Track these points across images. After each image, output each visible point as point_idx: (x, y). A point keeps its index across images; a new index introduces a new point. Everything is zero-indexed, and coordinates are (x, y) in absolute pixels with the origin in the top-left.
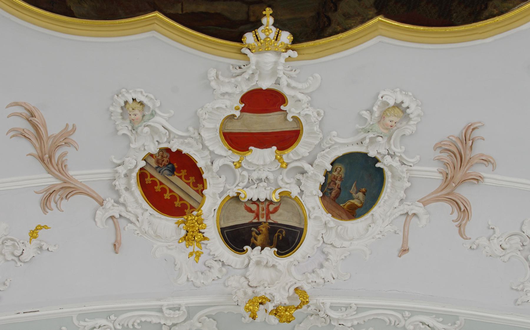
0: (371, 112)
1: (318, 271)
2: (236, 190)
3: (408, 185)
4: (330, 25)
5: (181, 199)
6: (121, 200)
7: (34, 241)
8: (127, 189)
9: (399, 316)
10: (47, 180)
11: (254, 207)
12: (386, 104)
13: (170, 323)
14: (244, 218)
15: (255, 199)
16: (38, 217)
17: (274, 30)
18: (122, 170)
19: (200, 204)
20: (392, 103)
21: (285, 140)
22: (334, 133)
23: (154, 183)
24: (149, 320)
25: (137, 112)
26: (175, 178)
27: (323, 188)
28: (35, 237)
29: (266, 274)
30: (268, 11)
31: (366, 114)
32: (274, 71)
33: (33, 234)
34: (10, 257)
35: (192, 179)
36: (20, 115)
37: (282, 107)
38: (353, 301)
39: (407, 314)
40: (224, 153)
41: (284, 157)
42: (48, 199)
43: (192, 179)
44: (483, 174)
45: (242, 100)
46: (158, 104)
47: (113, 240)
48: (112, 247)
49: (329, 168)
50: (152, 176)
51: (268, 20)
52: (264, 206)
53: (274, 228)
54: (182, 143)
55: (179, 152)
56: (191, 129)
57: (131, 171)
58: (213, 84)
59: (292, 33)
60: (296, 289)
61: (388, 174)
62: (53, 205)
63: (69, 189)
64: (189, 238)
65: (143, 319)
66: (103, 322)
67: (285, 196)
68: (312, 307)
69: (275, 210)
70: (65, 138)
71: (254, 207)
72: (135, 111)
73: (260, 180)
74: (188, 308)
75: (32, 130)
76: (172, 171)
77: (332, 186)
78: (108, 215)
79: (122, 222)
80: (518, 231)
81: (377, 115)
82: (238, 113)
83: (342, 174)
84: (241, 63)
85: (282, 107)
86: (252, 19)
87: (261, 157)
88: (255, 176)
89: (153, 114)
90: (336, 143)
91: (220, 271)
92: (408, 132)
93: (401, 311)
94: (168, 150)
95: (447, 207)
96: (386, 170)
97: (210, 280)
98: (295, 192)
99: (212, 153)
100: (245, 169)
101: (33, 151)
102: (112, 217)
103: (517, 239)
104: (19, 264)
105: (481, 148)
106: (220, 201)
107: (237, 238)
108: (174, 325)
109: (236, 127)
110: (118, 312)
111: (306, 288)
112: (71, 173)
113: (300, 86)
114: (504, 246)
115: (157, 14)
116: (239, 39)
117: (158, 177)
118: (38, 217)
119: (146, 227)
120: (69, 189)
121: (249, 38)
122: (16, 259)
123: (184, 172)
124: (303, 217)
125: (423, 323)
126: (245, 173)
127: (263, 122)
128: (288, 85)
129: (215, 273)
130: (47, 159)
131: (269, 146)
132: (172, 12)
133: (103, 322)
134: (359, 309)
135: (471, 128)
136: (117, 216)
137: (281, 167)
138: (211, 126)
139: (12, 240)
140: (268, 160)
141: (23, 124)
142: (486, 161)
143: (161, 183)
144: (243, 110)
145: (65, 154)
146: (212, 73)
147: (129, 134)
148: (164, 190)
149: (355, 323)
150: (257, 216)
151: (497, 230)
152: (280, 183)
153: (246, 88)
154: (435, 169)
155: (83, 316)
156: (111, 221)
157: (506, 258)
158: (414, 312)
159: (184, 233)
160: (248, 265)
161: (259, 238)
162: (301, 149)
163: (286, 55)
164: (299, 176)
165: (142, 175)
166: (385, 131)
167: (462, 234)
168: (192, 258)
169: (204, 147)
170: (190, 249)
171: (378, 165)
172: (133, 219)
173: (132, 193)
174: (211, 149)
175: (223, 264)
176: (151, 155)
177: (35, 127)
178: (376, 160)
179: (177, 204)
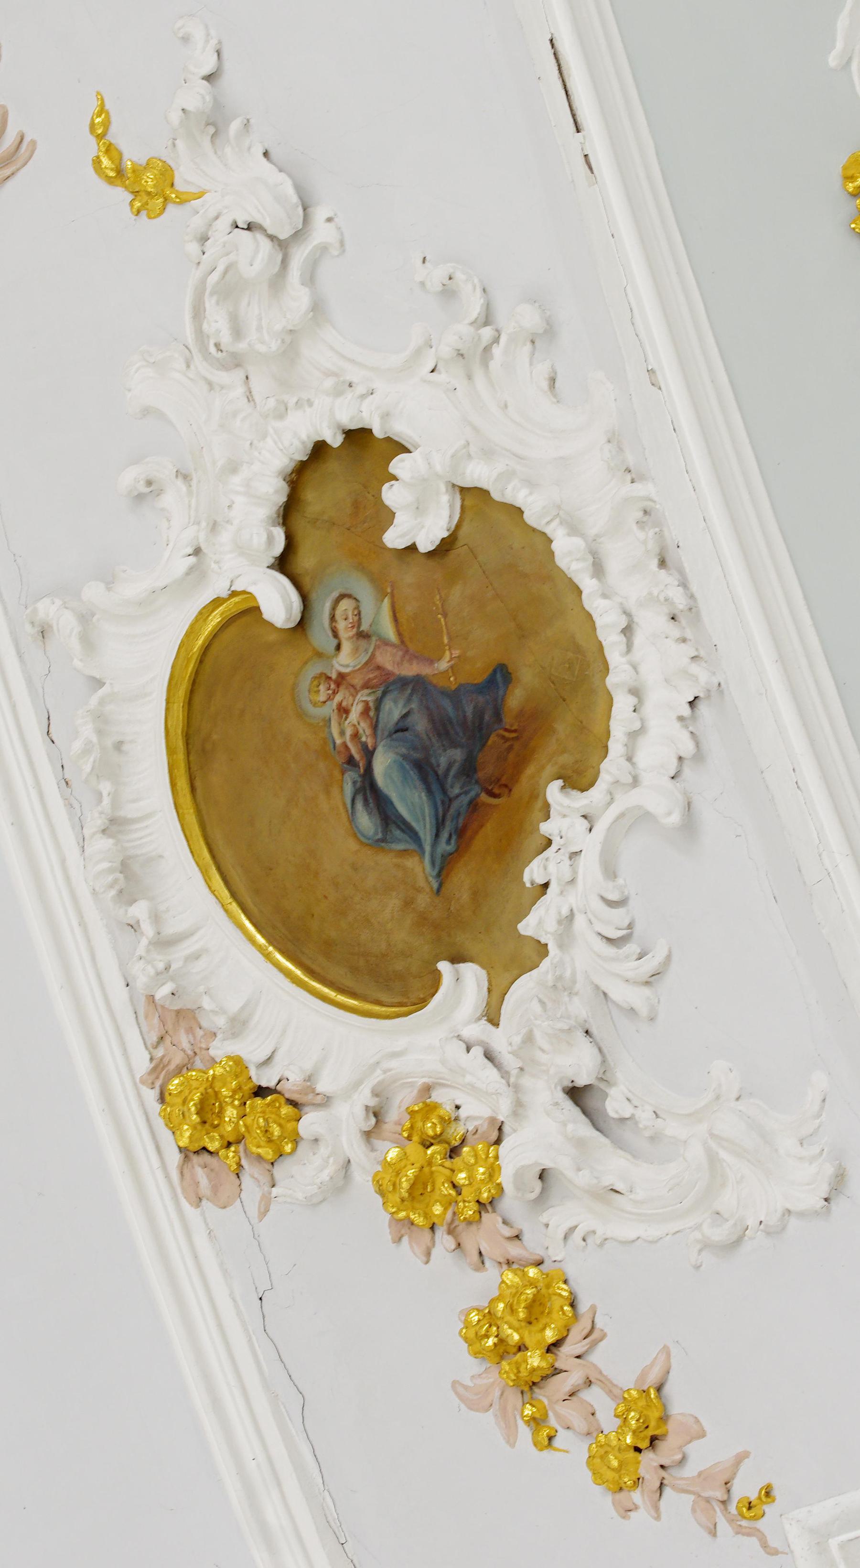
7: (186, 176)
28: (166, 175)
33: (150, 189)
34: (298, 297)
104: (322, 233)
122: (299, 256)
139: (198, 313)
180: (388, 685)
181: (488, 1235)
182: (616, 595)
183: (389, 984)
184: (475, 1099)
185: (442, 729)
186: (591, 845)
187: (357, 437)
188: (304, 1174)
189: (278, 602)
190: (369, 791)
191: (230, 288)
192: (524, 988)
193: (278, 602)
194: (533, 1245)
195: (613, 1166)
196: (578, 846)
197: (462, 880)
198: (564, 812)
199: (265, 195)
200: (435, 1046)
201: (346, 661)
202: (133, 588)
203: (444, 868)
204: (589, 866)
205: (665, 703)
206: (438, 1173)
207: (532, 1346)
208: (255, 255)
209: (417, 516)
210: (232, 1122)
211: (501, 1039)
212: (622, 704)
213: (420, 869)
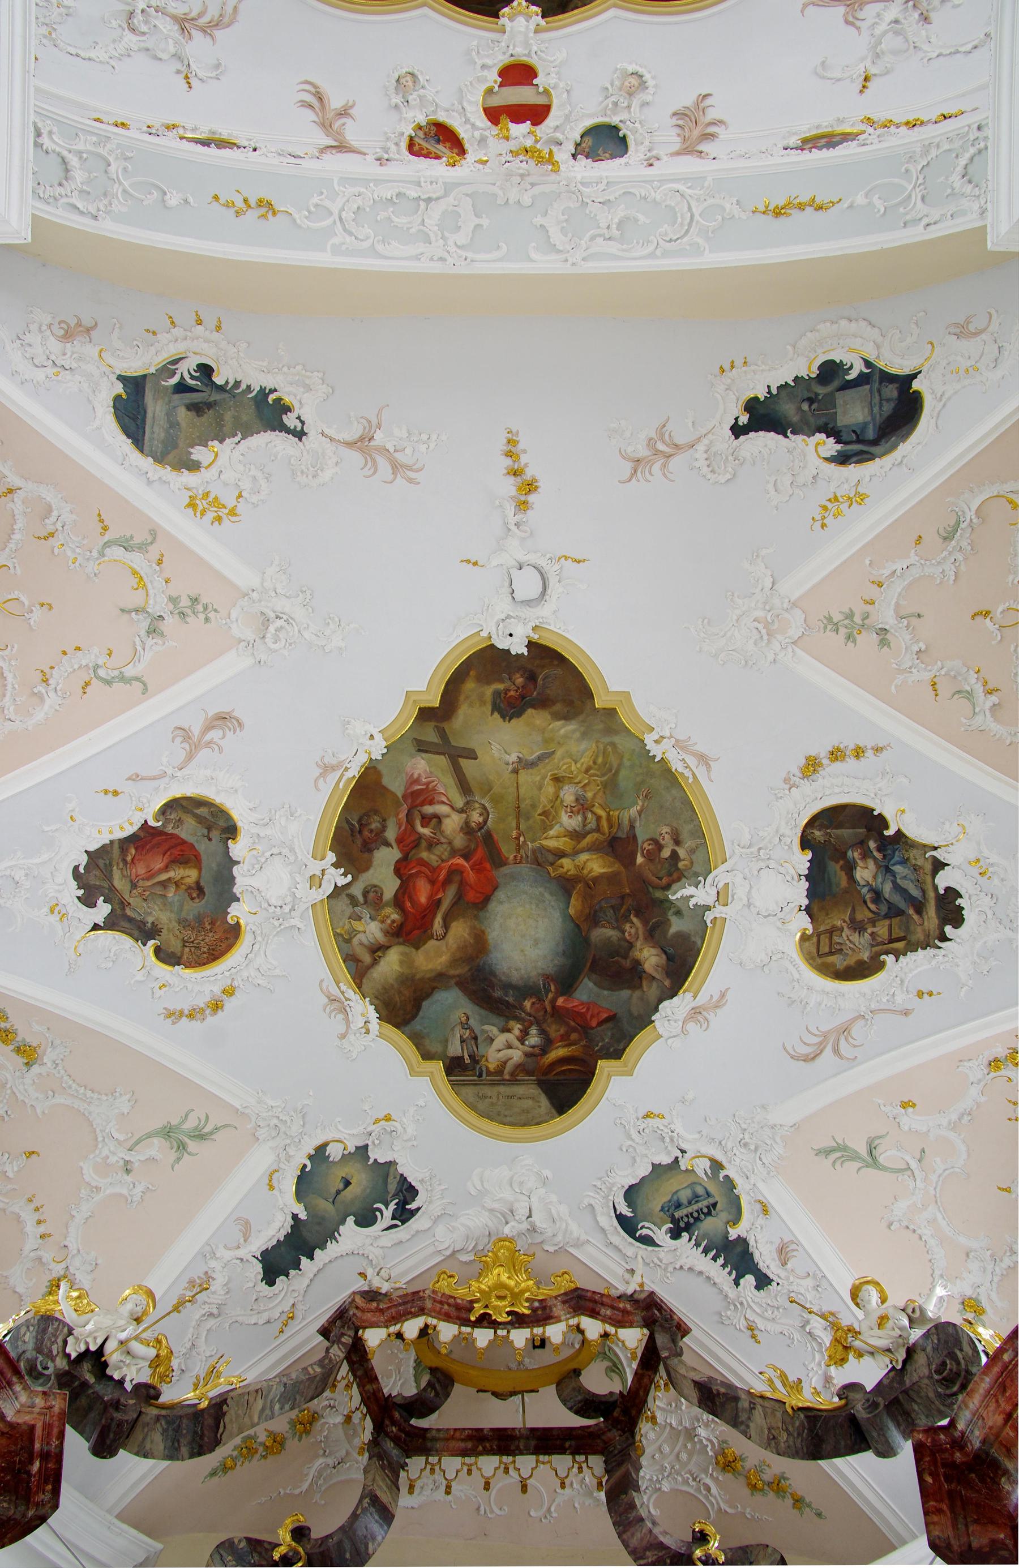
26: (440, 147)
37: (535, 82)
45: (501, 74)
74: (445, 183)
76: (438, 142)
82: (496, 88)
83: (590, 143)
101: (316, 119)
109: (496, 102)
116: (496, 16)
130: (326, 126)
144: (501, 85)
155: (345, 181)
162: (551, 121)
176: (420, 128)
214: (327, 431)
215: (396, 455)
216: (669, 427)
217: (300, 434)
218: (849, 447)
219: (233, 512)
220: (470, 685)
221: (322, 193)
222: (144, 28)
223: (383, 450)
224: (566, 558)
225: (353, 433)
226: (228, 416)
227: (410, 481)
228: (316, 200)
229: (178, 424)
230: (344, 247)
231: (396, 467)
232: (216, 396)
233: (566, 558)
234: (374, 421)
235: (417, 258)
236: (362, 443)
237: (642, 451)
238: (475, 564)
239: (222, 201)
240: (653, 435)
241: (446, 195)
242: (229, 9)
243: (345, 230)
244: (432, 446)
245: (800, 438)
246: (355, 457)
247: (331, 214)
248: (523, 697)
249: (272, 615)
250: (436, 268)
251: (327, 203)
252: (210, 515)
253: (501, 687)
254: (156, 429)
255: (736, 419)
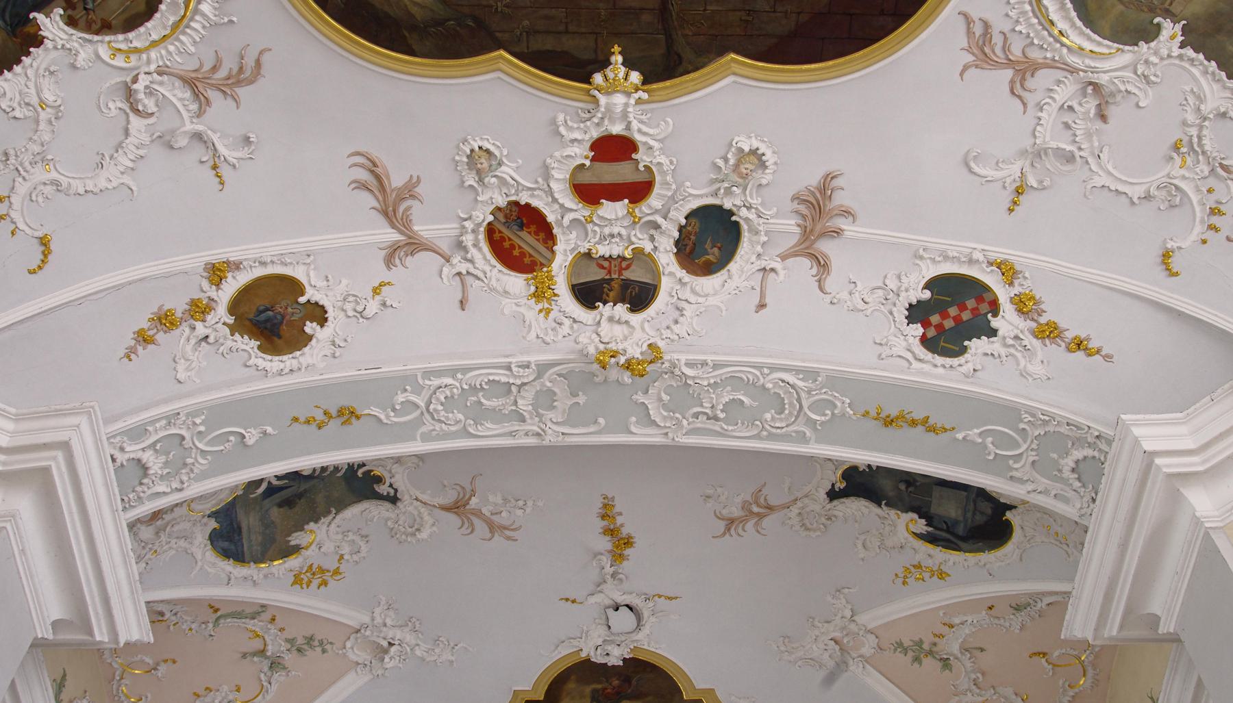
0: (726, 160)
1: (674, 327)
2: (587, 246)
3: (766, 239)
4: (681, 63)
5: (531, 256)
6: (469, 256)
7: (377, 298)
8: (475, 245)
9: (758, 373)
10: (394, 236)
11: (606, 264)
12: (741, 150)
13: (519, 382)
14: (595, 274)
15: (607, 256)
16: (383, 274)
17: (622, 70)
18: (469, 225)
19: (551, 261)
20: (747, 149)
21: (638, 191)
22: (688, 184)
23: (503, 239)
24: (497, 378)
25: (483, 160)
26: (524, 234)
27: (677, 243)
29: (619, 330)
30: (616, 49)
31: (721, 163)
32: (625, 114)
33: (376, 291)
34: (351, 313)
35: (542, 235)
36: (362, 166)
37: (634, 156)
38: (709, 358)
39: (766, 371)
40: (574, 207)
41: (637, 211)
42: (392, 255)
43: (542, 235)
44: (843, 227)
45: (592, 148)
46: (505, 153)
47: (459, 297)
48: (458, 305)
49: (683, 222)
50: (500, 232)
51: (618, 59)
52: (617, 263)
53: (627, 284)
54: (532, 196)
55: (528, 205)
56: (540, 180)
57: (479, 225)
58: (562, 130)
59: (642, 73)
60: (650, 345)
61: (744, 226)
62: (397, 261)
63: (414, 245)
64: (538, 295)
65: (491, 378)
66: (449, 381)
67: (638, 252)
68: (667, 365)
69: (628, 267)
70: (409, 191)
71: (606, 264)
72: (480, 162)
73: (612, 236)
75: (375, 182)
77: (686, 241)
78: (454, 271)
79: (469, 280)
80: (881, 284)
81: (732, 162)
82: (588, 163)
84: (590, 106)
85: (634, 156)
86: (601, 57)
87: (613, 210)
88: (607, 231)
89: (500, 164)
90: (690, 195)
91: (572, 328)
92: (764, 182)
93: (759, 367)
94: (516, 203)
95: (806, 262)
96: (742, 222)
97: (560, 337)
98: (648, 247)
99: (562, 206)
100: (596, 224)
101: (377, 205)
102: (459, 274)
103: (880, 293)
105: (840, 199)
106: (570, 258)
107: (588, 295)
108: (524, 384)
109: (586, 178)
110: (465, 370)
111: (661, 344)
112: (416, 228)
113: (651, 131)
114: (867, 300)
115: (502, 52)
116: (587, 79)
117: (507, 233)
118: (383, 274)
119: (494, 282)
120: (414, 245)
121: (598, 78)
123: (533, 228)
124: (657, 274)
125: (783, 381)
126: (596, 228)
127: (614, 171)
128: (640, 131)
129: (566, 329)
131: (621, 199)
132: (517, 50)
133: (449, 381)
134: (716, 366)
135: (829, 177)
136: (464, 272)
137: (634, 222)
138: (561, 176)
140: (620, 215)
141: (364, 175)
142: (847, 213)
143: (510, 239)
144: (593, 159)
145: (408, 208)
146: (561, 117)
147: (476, 185)
148: (513, 247)
149: (712, 381)
150: (609, 272)
151: (859, 284)
152: (633, 239)
153: (595, 134)
154: (793, 222)
155: (428, 374)
156: (457, 278)
157: (868, 312)
158: (774, 369)
159: (533, 289)
160: (599, 322)
161: (611, 294)
162: (654, 201)
163: (636, 96)
164: (652, 232)
165: (491, 231)
166: (740, 180)
167: (821, 289)
168: (542, 315)
169: (555, 200)
170: (540, 306)
171: (734, 218)
172: (481, 275)
173: (480, 249)
174: (561, 201)
175: (575, 321)
176: (499, 209)
177: (378, 178)
178: (730, 213)
179: (527, 260)
180: (283, 317)
181: (187, 316)
182: (288, 361)
183: (234, 307)
184: (211, 318)
185: (274, 325)
186: (247, 348)
187: (326, 320)
188: (205, 284)
189: (302, 300)
190: (267, 309)
191: (358, 303)
192: (228, 331)
193: (302, 300)
194: (184, 324)
195: (193, 341)
196: (249, 345)
197: (247, 323)
198: (255, 343)
199: (369, 312)
200: (221, 312)
201: (290, 310)
202: (312, 273)
203: (251, 320)
204: (244, 347)
205: (268, 365)
206: (199, 310)
207: (165, 321)
208: (360, 308)
209: (310, 327)
210: (216, 273)
211: (220, 325)
212: (269, 357)
213: (251, 316)
214: (421, 497)
215: (494, 518)
216: (764, 491)
217: (393, 499)
218: (938, 532)
219: (337, 572)
220: (571, 685)
221: (406, 390)
222: (152, 108)
223: (478, 513)
224: (660, 596)
225: (449, 497)
226: (320, 498)
227: (509, 538)
228: (401, 398)
229: (273, 522)
230: (434, 433)
231: (493, 527)
232: (304, 486)
233: (660, 596)
234: (468, 488)
235: (511, 434)
236: (457, 507)
237: (736, 512)
238: (574, 601)
239: (302, 420)
240: (749, 498)
241: (539, 376)
242: (250, 62)
243: (433, 418)
244: (528, 510)
245: (893, 513)
246: (452, 518)
247: (417, 406)
248: (618, 693)
249: (385, 644)
250: (531, 441)
251: (413, 398)
252: (316, 582)
253: (599, 686)
254: (253, 537)
255: (833, 485)
